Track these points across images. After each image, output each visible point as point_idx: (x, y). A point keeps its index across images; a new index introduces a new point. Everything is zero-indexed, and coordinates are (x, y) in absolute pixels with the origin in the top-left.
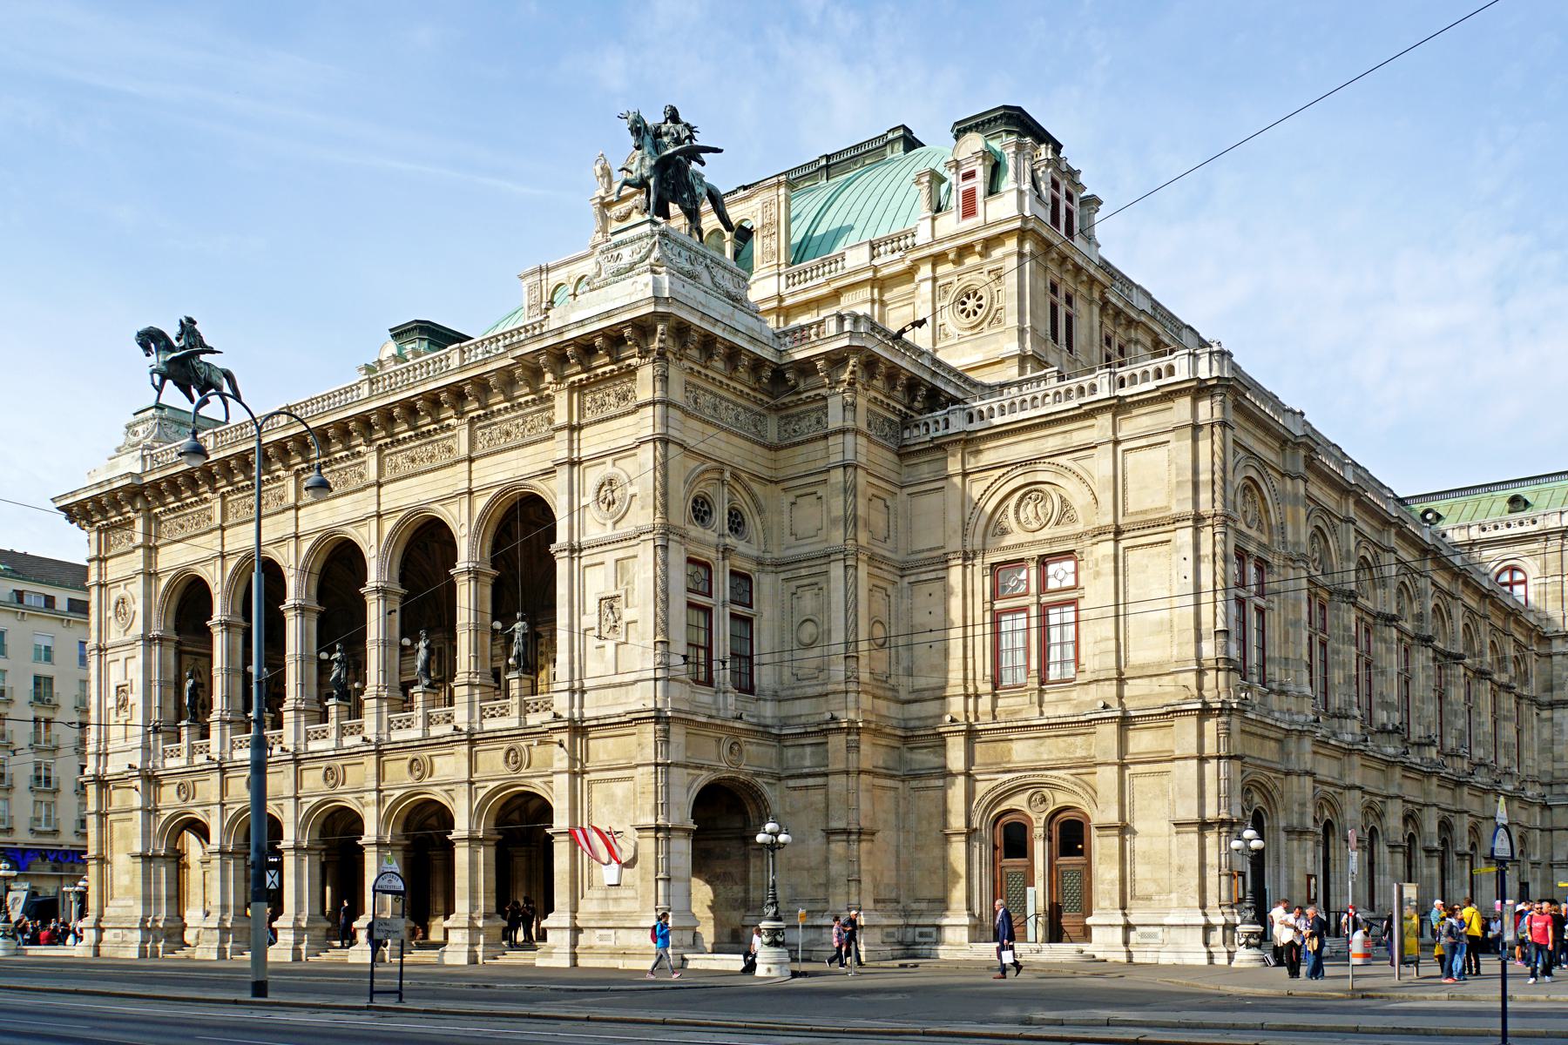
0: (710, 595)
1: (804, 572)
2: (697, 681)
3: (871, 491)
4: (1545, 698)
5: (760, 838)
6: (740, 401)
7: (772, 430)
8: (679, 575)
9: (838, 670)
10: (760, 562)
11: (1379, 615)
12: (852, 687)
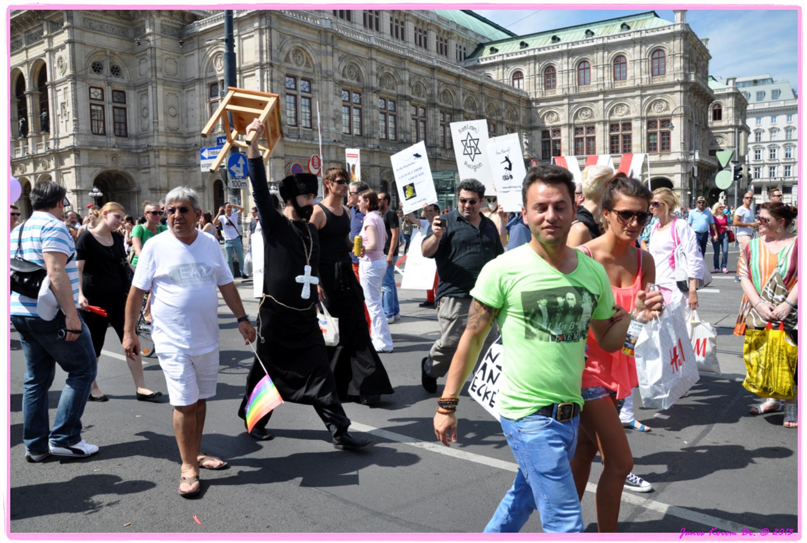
0: (103, 100)
1: (142, 89)
2: (94, 134)
3: (165, 57)
4: (529, 125)
6: (113, 23)
7: (131, 33)
8: (82, 94)
9: (151, 128)
10: (128, 86)
11: (398, 95)
12: (156, 133)
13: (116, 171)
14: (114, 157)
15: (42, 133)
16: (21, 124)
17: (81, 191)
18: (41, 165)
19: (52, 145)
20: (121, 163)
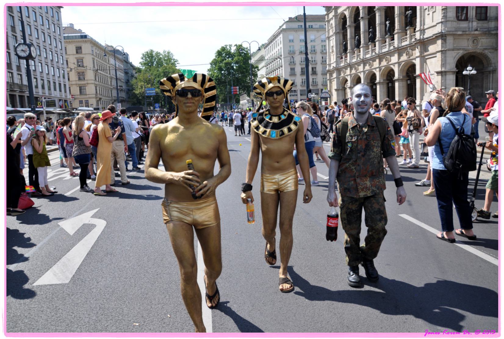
5: (465, 73)
13: (475, 52)
14: (475, 40)
15: (408, 28)
16: (388, 25)
17: (445, 72)
18: (405, 55)
19: (418, 35)
20: (480, 45)
